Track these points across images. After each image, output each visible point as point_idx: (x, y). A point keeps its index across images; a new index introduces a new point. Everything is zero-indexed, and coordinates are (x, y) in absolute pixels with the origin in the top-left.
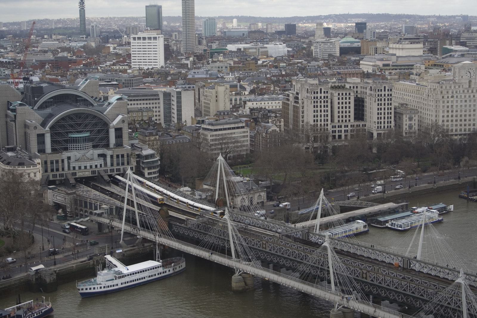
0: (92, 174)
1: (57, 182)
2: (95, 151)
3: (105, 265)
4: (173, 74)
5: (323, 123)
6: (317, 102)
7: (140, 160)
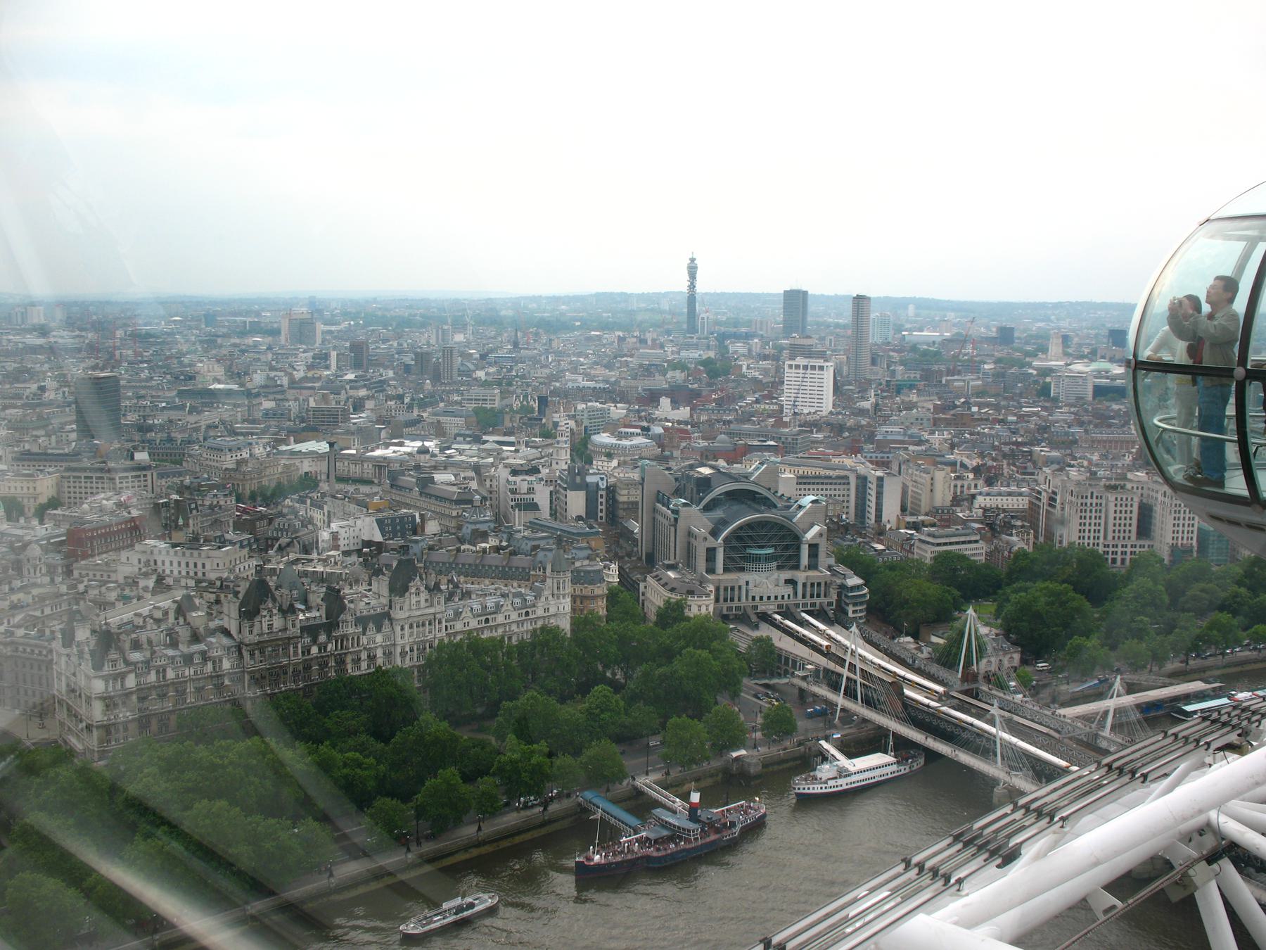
3: (824, 757)
5: (1091, 541)
6: (1085, 511)
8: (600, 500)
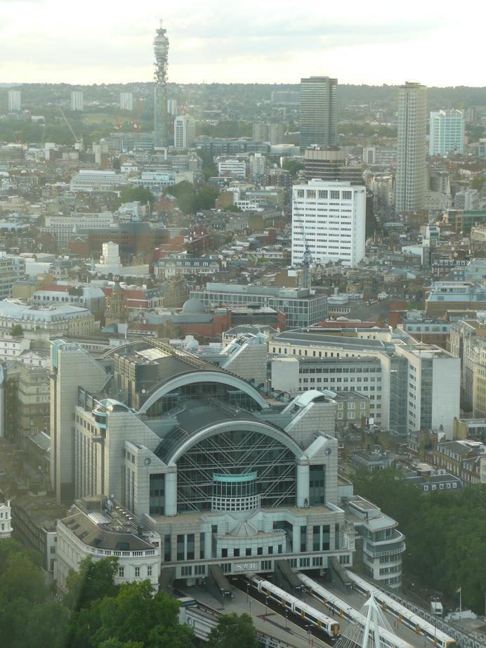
0: (262, 568)
1: (189, 584)
2: (267, 515)
7: (362, 540)
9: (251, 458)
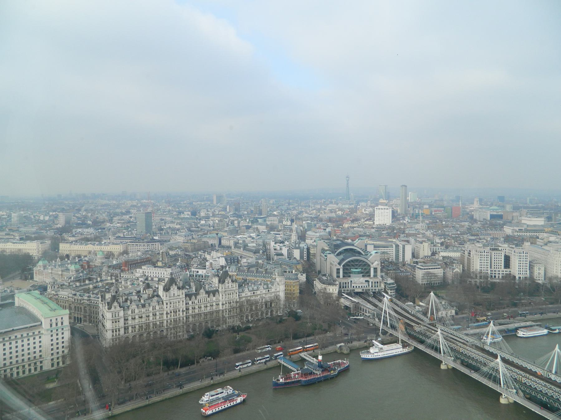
4: (397, 229)
5: (485, 269)
6: (482, 258)
8: (305, 253)
9: (360, 265)
